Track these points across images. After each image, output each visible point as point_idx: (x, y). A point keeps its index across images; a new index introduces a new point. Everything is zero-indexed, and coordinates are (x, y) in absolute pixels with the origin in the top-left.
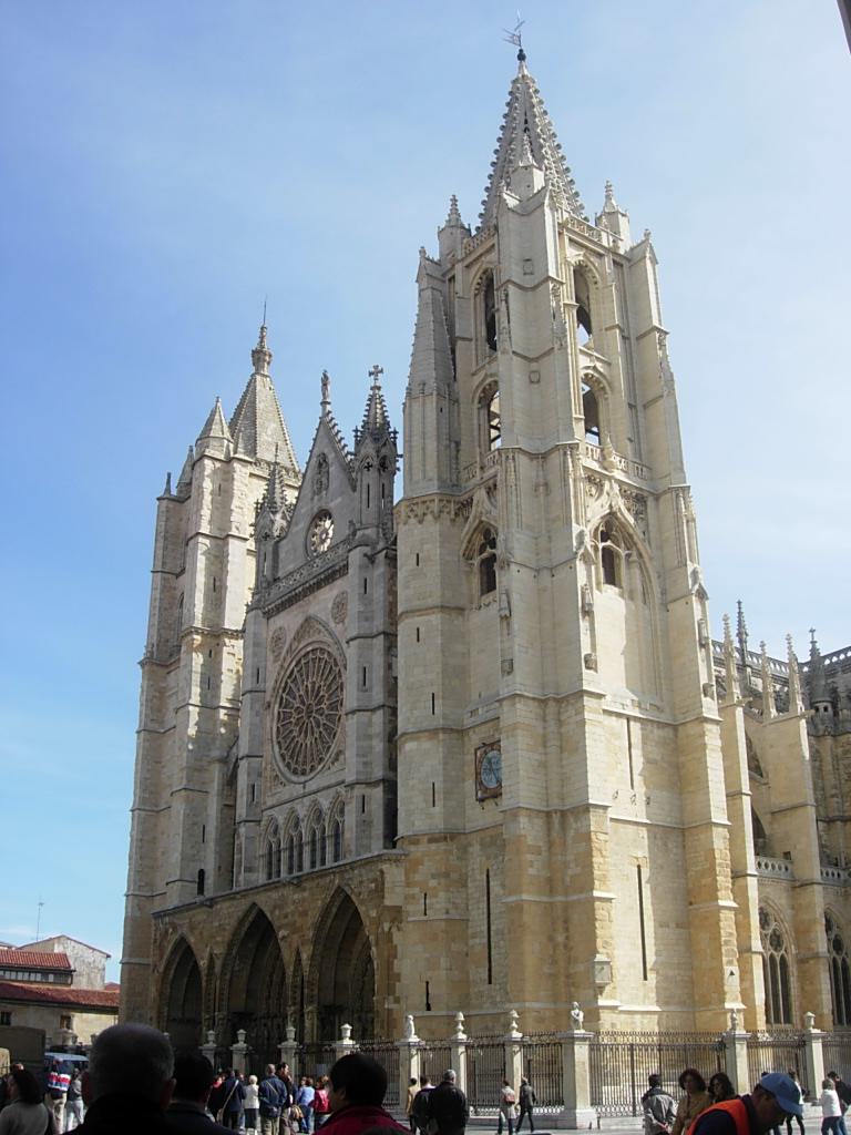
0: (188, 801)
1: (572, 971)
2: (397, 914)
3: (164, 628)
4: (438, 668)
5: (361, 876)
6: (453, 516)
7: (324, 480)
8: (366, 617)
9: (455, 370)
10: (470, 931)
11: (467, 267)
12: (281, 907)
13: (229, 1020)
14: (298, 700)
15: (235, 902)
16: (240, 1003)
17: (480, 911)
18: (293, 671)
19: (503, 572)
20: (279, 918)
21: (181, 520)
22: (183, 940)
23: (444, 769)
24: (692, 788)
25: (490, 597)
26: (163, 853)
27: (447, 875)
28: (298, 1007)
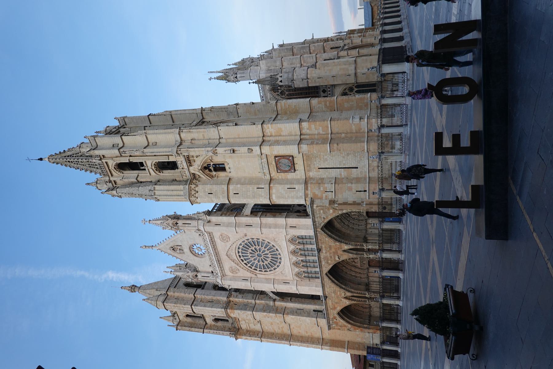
0: (288, 314)
1: (355, 132)
2: (332, 202)
3: (225, 329)
4: (248, 186)
5: (318, 217)
6: (197, 181)
7: (179, 248)
8: (228, 225)
9: (147, 182)
10: (339, 177)
11: (112, 176)
12: (328, 259)
13: (369, 291)
14: (255, 261)
15: (325, 284)
16: (363, 287)
17: (333, 172)
18: (245, 263)
19: (218, 153)
20: (331, 261)
21: (186, 322)
22: (338, 314)
23: (283, 184)
24: (298, 109)
25: (227, 168)
26: (307, 332)
27: (319, 184)
28: (364, 253)
